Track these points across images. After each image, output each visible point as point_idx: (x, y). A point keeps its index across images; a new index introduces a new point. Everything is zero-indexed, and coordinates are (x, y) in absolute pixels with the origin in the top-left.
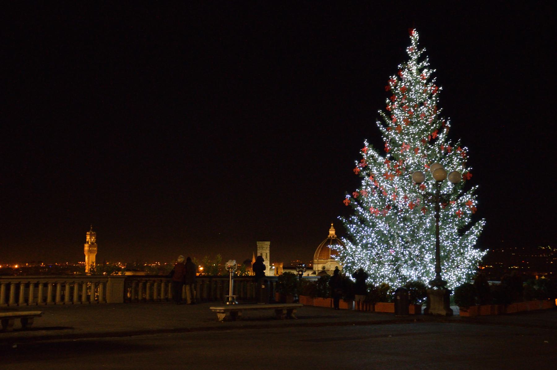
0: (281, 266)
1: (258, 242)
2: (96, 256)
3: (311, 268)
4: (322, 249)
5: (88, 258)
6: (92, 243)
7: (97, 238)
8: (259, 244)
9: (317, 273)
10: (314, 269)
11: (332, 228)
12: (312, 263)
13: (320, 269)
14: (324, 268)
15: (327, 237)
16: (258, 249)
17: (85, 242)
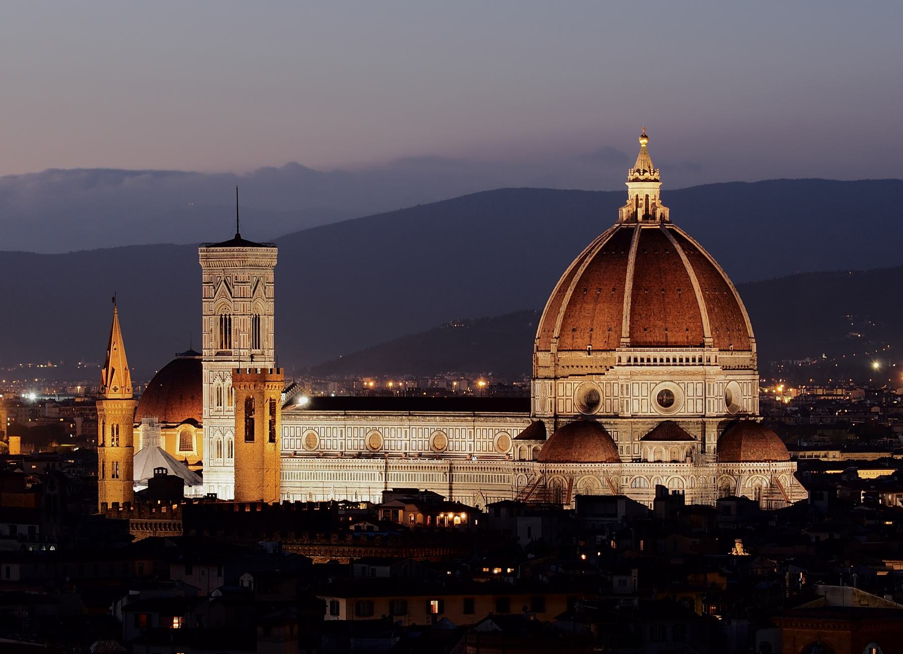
9: (549, 428)
14: (591, 401)
16: (207, 290)
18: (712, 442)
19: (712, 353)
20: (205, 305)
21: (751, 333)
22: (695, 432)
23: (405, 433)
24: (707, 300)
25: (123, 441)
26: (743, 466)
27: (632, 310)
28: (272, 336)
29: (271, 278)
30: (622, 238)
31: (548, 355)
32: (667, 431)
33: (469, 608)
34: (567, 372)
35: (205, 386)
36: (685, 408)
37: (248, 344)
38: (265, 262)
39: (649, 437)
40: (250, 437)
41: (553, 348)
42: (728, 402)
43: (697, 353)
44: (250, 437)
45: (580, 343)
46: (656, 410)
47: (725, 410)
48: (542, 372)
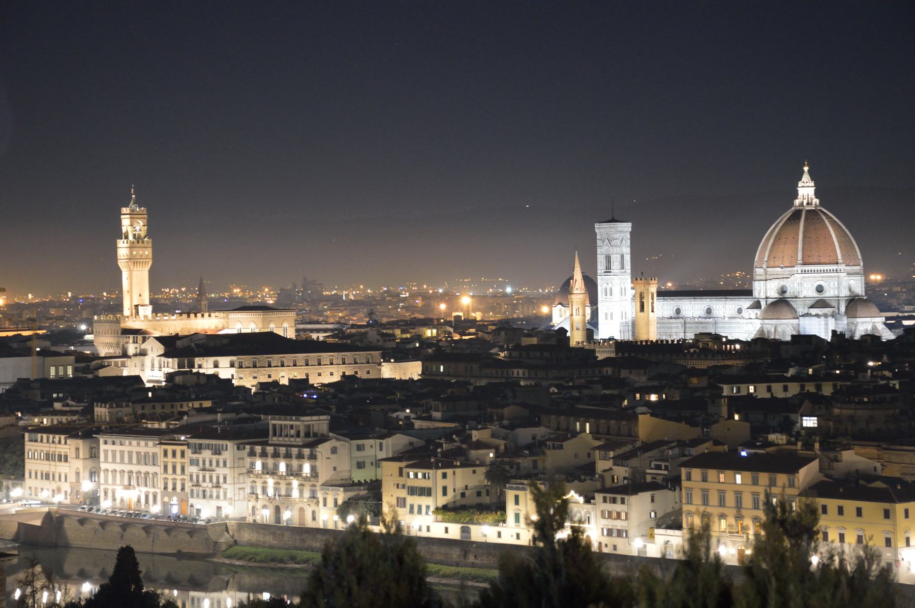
0: (653, 289)
1: (597, 225)
2: (151, 272)
3: (748, 293)
4: (778, 238)
5: (130, 277)
6: (137, 238)
7: (150, 224)
8: (602, 230)
10: (756, 294)
11: (806, 177)
12: (752, 280)
13: (774, 294)
14: (783, 291)
15: (792, 204)
17: (118, 233)
18: (843, 309)
19: (842, 267)
20: (599, 250)
21: (860, 257)
22: (834, 304)
23: (693, 308)
24: (839, 242)
25: (581, 313)
26: (858, 320)
27: (803, 248)
28: (629, 264)
29: (629, 236)
30: (797, 215)
31: (762, 270)
32: (821, 303)
33: (786, 389)
34: (771, 277)
35: (599, 287)
36: (830, 292)
37: (619, 267)
38: (626, 229)
39: (812, 307)
40: (642, 309)
41: (764, 266)
42: (850, 290)
43: (835, 267)
44: (642, 309)
45: (777, 263)
46: (815, 294)
47: (848, 294)
48: (758, 278)
